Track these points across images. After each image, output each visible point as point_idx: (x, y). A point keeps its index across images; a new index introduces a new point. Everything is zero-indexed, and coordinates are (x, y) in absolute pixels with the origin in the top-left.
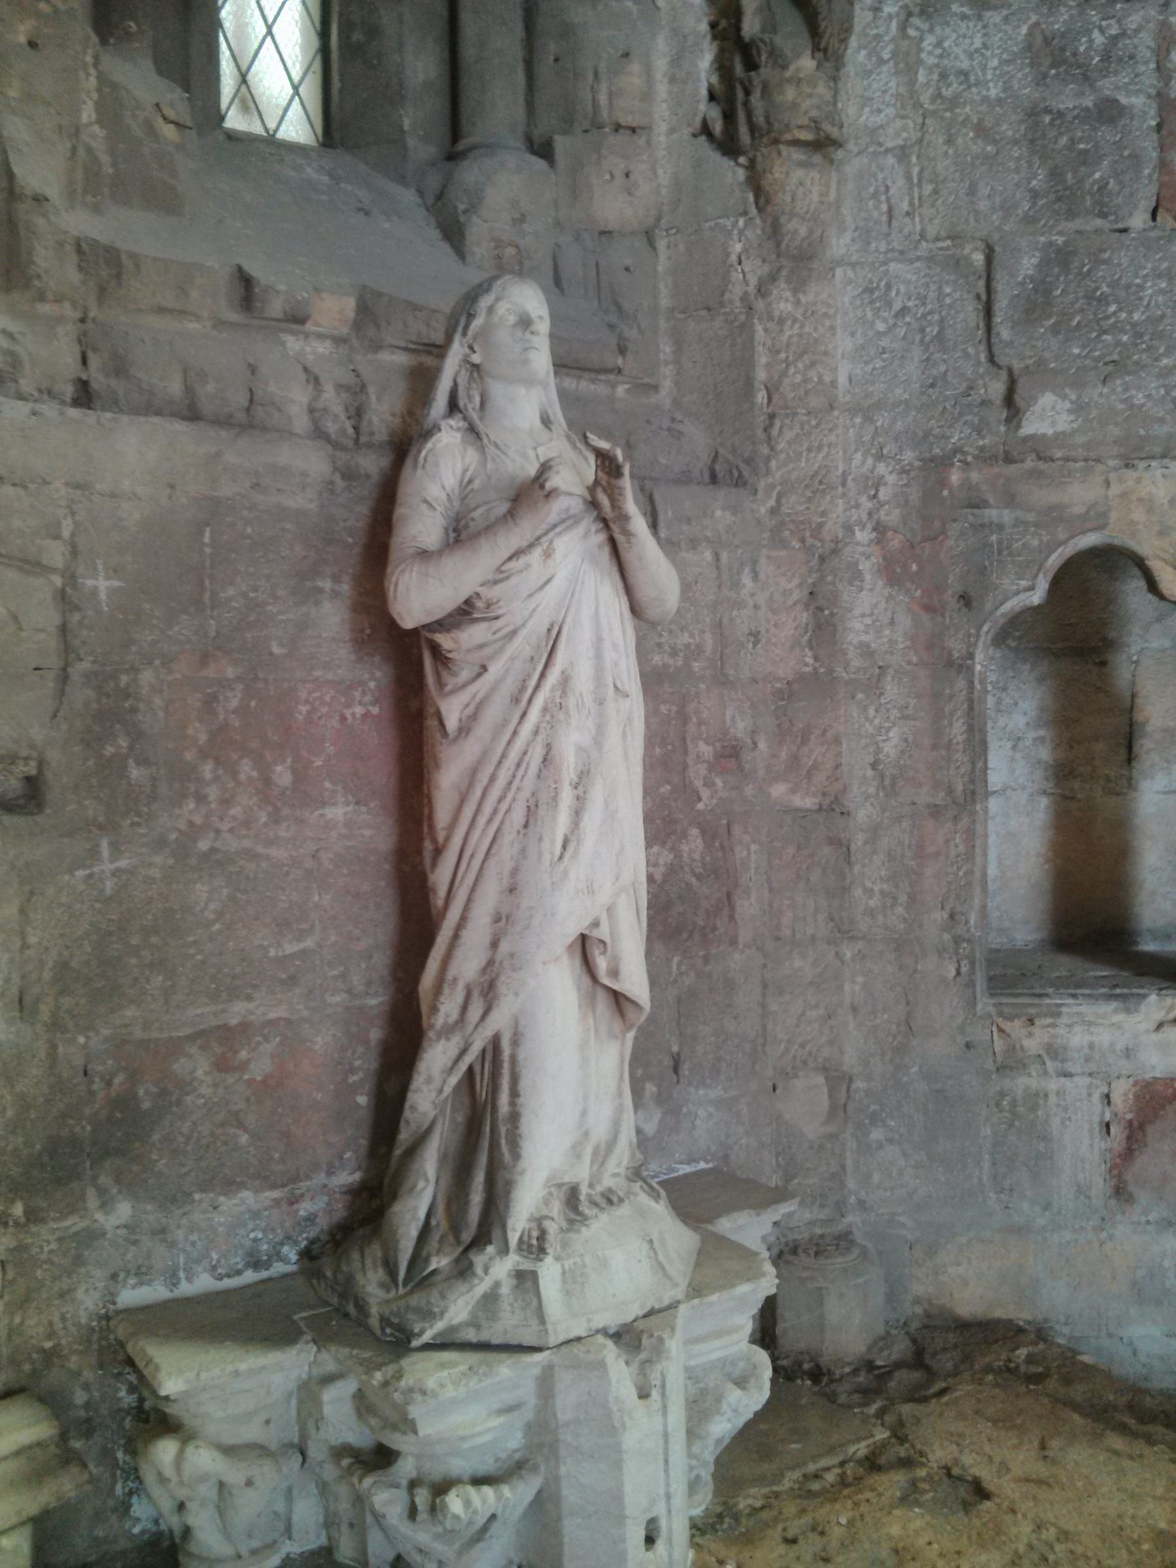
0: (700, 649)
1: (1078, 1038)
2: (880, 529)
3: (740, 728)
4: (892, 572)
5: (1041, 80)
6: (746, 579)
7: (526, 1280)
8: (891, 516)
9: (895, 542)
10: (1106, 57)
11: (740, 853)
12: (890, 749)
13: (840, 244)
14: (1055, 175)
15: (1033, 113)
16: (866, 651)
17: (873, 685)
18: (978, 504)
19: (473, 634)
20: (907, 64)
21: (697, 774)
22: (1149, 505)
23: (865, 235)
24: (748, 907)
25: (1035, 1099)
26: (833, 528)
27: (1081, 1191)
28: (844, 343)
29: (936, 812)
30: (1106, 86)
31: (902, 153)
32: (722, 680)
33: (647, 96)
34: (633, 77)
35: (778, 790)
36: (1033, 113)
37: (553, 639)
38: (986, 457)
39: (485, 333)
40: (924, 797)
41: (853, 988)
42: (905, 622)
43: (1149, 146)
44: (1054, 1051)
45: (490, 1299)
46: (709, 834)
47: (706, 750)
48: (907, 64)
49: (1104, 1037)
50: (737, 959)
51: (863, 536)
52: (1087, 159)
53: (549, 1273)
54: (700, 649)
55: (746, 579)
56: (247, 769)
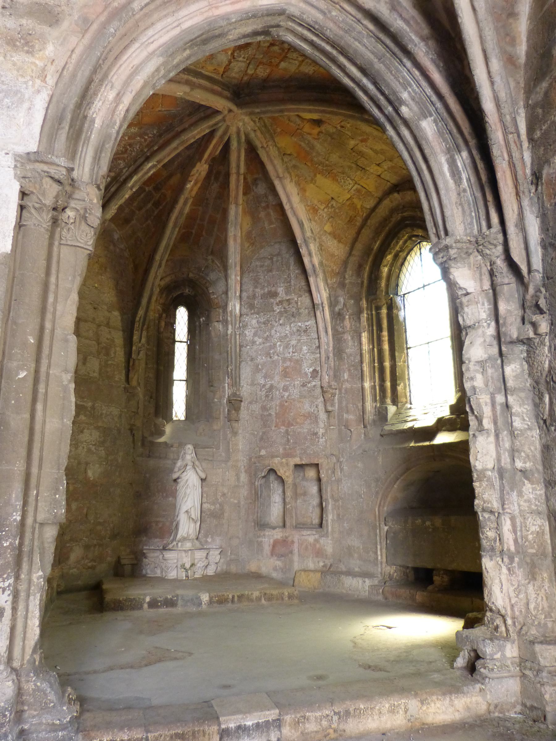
0: (219, 482)
1: (267, 533)
2: (245, 466)
3: (226, 491)
4: (246, 472)
5: (262, 411)
6: (227, 473)
7: (177, 544)
8: (246, 465)
9: (246, 468)
10: (270, 408)
11: (225, 507)
12: (245, 495)
13: (240, 431)
14: (264, 423)
15: (261, 415)
16: (243, 482)
17: (244, 486)
18: (255, 463)
19: (180, 480)
20: (248, 409)
21: (219, 497)
22: (275, 463)
23: (243, 430)
24: (226, 515)
25: (261, 542)
26: (239, 466)
27: (267, 555)
28: (240, 444)
29: (251, 503)
30: (270, 412)
31: (247, 421)
32: (222, 485)
33: (220, 414)
34: (218, 412)
35: (232, 500)
36: (261, 415)
37: (187, 480)
38: (256, 457)
39: (185, 450)
40: (250, 501)
41: (241, 526)
42: (247, 478)
43: (274, 419)
44: (264, 535)
45: (173, 546)
46: (220, 505)
47: (220, 494)
48: (248, 409)
49: (270, 533)
50: (224, 521)
51: (242, 467)
52: (267, 421)
53: (180, 544)
54: (219, 482)
55: (227, 473)
56: (161, 494)
